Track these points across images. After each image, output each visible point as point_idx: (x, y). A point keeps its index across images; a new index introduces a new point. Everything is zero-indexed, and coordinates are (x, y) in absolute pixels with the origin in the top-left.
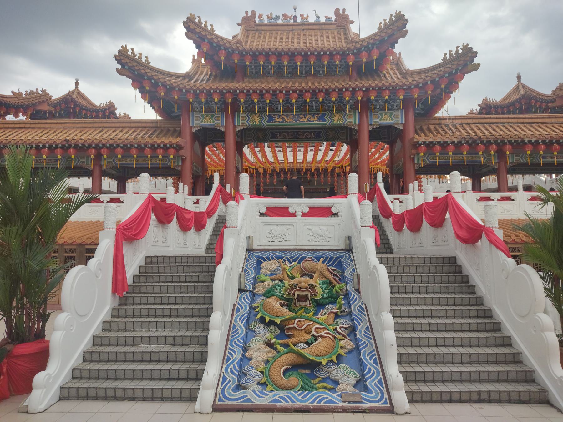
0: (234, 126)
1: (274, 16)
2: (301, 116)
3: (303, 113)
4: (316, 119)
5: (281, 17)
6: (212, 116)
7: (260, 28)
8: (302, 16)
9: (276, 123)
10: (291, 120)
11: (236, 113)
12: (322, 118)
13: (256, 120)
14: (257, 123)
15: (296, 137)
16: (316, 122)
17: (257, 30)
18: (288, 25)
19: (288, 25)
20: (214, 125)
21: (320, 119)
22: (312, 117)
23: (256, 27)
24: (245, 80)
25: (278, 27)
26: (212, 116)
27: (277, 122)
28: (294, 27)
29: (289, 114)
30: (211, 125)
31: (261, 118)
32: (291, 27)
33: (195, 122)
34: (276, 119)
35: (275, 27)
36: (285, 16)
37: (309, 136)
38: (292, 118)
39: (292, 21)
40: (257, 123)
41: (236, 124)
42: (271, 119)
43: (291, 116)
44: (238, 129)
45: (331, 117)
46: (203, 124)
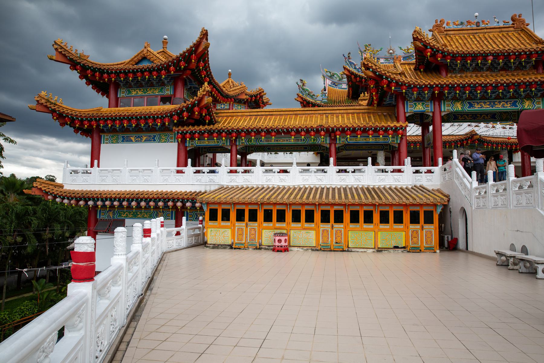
0: (441, 112)
1: (459, 23)
2: (496, 103)
3: (498, 101)
4: (509, 105)
5: (466, 23)
6: (423, 104)
7: (449, 32)
8: (483, 21)
9: (476, 109)
10: (488, 106)
11: (442, 101)
12: (514, 104)
13: (458, 107)
14: (460, 109)
15: (474, 119)
16: (510, 108)
17: (447, 34)
18: (472, 30)
19: (472, 30)
20: (424, 111)
21: (512, 105)
22: (505, 103)
23: (445, 32)
24: (449, 75)
25: (464, 32)
26: (423, 104)
27: (477, 108)
28: (477, 31)
29: (486, 101)
30: (422, 111)
31: (463, 106)
32: (475, 31)
33: (409, 109)
34: (476, 106)
35: (461, 32)
36: (469, 22)
37: (486, 118)
38: (489, 105)
39: (474, 27)
40: (460, 109)
41: (443, 110)
42: (471, 105)
43: (488, 103)
44: (443, 114)
45: (522, 103)
46: (416, 110)
